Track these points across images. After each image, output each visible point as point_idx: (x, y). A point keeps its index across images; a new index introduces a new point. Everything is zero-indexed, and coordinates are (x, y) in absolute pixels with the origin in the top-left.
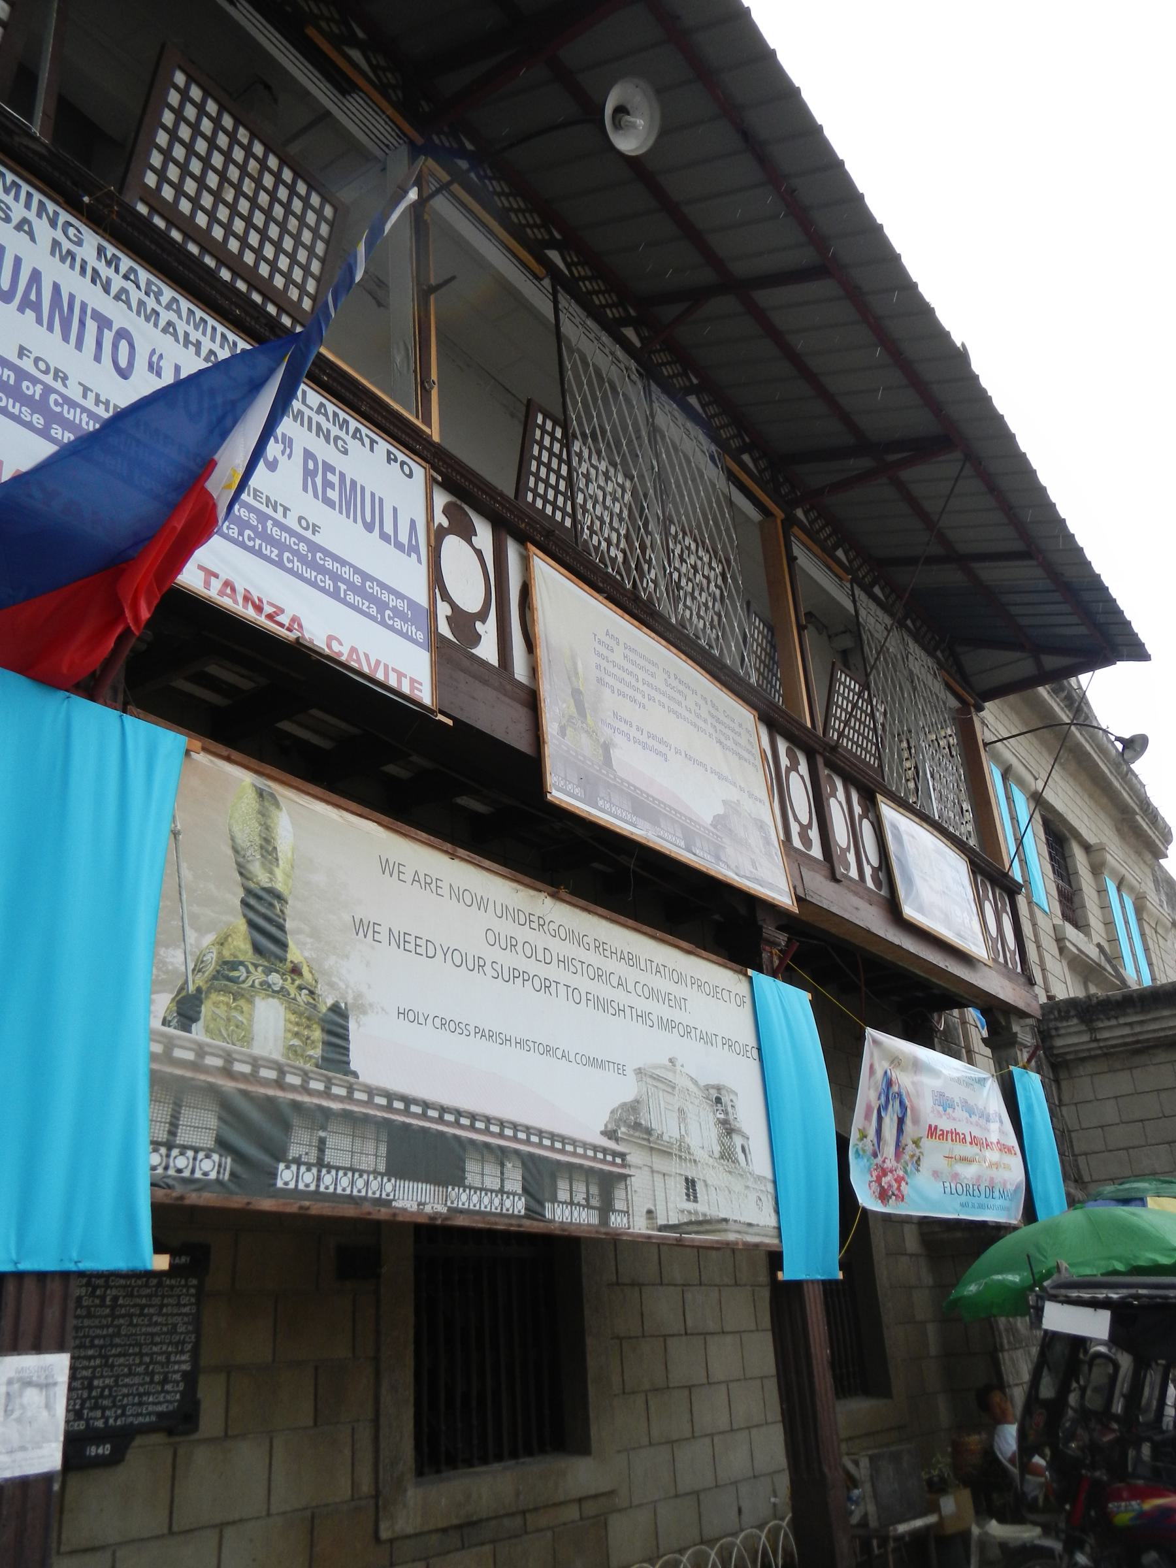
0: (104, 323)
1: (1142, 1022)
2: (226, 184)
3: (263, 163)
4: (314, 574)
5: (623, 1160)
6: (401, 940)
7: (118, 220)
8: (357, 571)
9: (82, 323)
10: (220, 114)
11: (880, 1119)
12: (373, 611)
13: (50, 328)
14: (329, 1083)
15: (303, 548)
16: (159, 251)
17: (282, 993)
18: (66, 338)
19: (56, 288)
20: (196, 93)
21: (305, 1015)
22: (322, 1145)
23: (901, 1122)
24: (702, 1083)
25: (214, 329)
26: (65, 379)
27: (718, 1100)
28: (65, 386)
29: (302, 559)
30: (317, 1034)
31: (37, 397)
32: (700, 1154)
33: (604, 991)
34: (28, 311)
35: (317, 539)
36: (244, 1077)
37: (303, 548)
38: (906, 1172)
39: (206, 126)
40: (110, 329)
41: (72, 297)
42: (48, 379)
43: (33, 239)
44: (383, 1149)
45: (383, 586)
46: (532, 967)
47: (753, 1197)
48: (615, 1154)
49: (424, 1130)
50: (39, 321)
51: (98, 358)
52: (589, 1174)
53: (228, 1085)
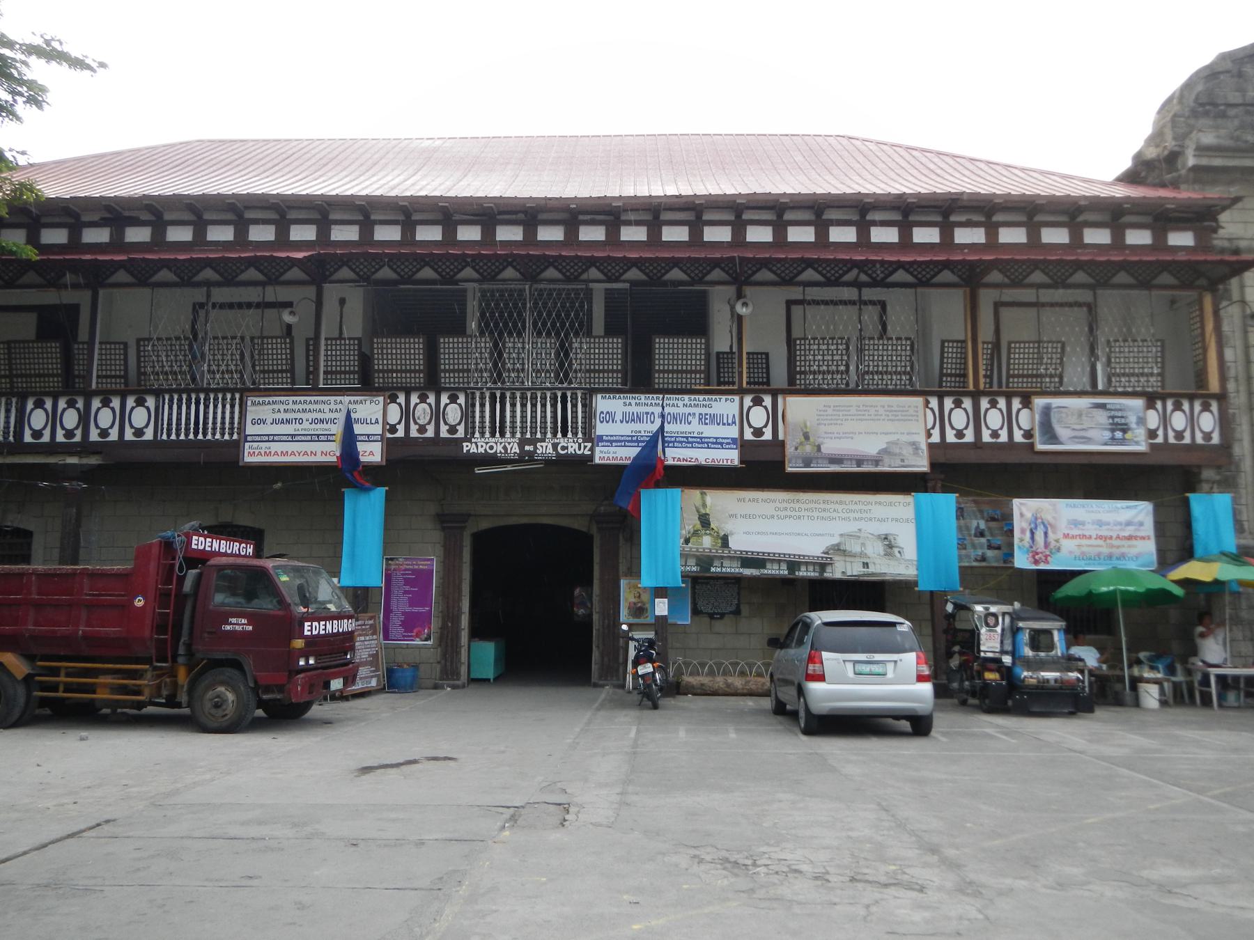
6: (744, 516)
15: (699, 440)
22: (722, 563)
23: (1046, 534)
24: (876, 534)
29: (698, 443)
30: (720, 541)
33: (828, 514)
35: (703, 435)
44: (739, 563)
45: (722, 438)
46: (793, 514)
48: (827, 558)
52: (814, 564)
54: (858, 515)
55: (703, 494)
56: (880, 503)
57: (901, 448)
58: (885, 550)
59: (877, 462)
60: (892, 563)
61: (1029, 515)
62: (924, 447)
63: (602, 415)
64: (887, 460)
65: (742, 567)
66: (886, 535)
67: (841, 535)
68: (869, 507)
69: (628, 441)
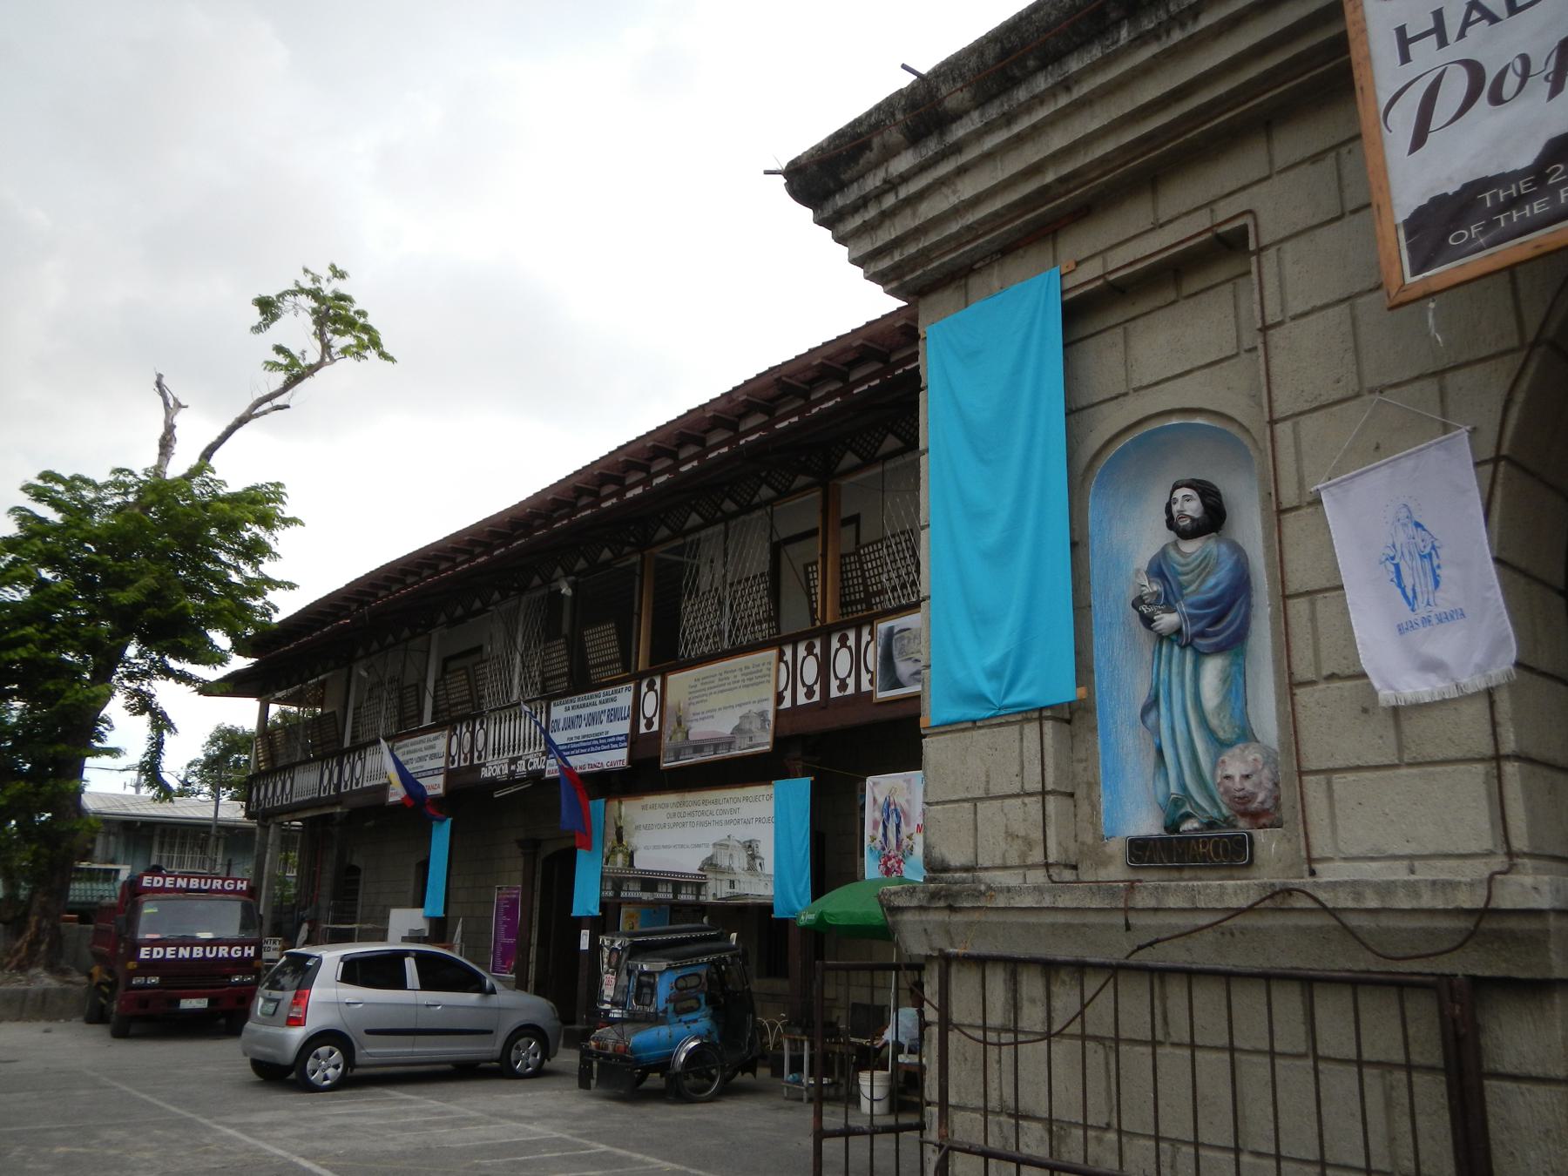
11: (885, 827)
21: (626, 855)
27: (750, 846)
32: (737, 870)
33: (704, 818)
38: (904, 856)
46: (680, 820)
47: (763, 884)
48: (702, 876)
52: (692, 884)
54: (728, 817)
55: (620, 802)
56: (746, 799)
57: (751, 723)
58: (748, 863)
59: (729, 743)
60: (755, 880)
61: (881, 800)
62: (771, 716)
64: (738, 742)
65: (643, 890)
66: (750, 841)
67: (714, 845)
68: (738, 805)
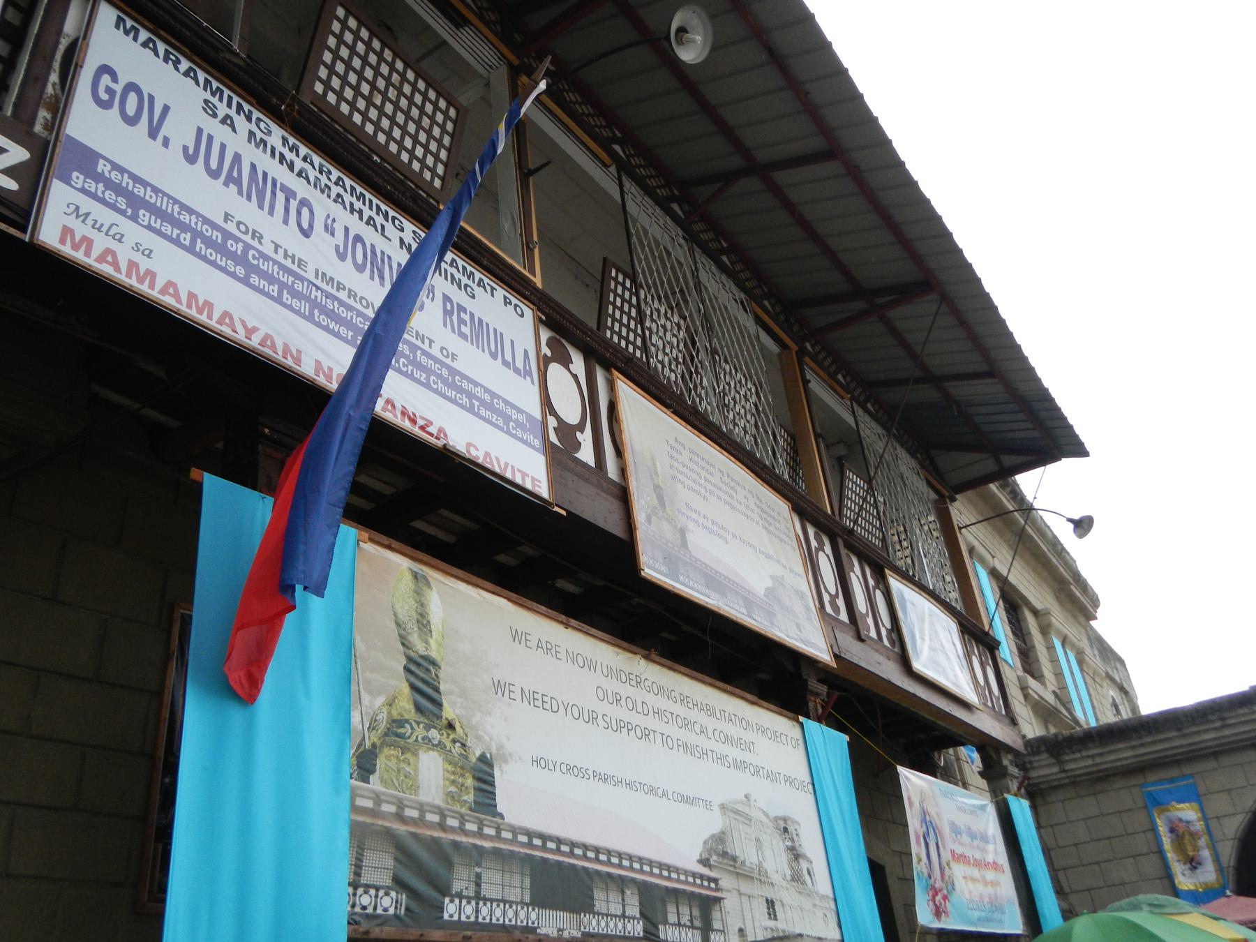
0: (289, 194)
1: (1101, 755)
2: (375, 92)
3: (403, 76)
4: (454, 393)
5: (717, 884)
6: (531, 698)
7: (298, 117)
8: (487, 390)
9: (274, 194)
10: (370, 39)
12: (501, 423)
13: (249, 198)
14: (481, 825)
15: (445, 372)
16: (329, 140)
17: (440, 746)
18: (261, 207)
19: (253, 167)
20: (352, 23)
21: (459, 765)
24: (772, 814)
25: (371, 201)
26: (261, 237)
27: (786, 830)
28: (261, 243)
29: (445, 381)
30: (470, 782)
31: (239, 252)
32: (776, 878)
33: (691, 738)
34: (231, 185)
35: (455, 365)
36: (413, 822)
37: (445, 372)
39: (361, 47)
40: (295, 200)
41: (265, 175)
42: (248, 238)
43: (234, 131)
44: (527, 882)
45: (507, 403)
46: (635, 719)
47: (820, 913)
48: (710, 880)
49: (558, 863)
50: (240, 193)
51: (286, 222)
53: (400, 828)
63: (106, 80)
69: (209, 243)
